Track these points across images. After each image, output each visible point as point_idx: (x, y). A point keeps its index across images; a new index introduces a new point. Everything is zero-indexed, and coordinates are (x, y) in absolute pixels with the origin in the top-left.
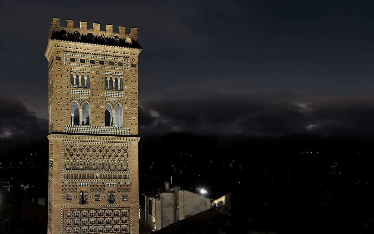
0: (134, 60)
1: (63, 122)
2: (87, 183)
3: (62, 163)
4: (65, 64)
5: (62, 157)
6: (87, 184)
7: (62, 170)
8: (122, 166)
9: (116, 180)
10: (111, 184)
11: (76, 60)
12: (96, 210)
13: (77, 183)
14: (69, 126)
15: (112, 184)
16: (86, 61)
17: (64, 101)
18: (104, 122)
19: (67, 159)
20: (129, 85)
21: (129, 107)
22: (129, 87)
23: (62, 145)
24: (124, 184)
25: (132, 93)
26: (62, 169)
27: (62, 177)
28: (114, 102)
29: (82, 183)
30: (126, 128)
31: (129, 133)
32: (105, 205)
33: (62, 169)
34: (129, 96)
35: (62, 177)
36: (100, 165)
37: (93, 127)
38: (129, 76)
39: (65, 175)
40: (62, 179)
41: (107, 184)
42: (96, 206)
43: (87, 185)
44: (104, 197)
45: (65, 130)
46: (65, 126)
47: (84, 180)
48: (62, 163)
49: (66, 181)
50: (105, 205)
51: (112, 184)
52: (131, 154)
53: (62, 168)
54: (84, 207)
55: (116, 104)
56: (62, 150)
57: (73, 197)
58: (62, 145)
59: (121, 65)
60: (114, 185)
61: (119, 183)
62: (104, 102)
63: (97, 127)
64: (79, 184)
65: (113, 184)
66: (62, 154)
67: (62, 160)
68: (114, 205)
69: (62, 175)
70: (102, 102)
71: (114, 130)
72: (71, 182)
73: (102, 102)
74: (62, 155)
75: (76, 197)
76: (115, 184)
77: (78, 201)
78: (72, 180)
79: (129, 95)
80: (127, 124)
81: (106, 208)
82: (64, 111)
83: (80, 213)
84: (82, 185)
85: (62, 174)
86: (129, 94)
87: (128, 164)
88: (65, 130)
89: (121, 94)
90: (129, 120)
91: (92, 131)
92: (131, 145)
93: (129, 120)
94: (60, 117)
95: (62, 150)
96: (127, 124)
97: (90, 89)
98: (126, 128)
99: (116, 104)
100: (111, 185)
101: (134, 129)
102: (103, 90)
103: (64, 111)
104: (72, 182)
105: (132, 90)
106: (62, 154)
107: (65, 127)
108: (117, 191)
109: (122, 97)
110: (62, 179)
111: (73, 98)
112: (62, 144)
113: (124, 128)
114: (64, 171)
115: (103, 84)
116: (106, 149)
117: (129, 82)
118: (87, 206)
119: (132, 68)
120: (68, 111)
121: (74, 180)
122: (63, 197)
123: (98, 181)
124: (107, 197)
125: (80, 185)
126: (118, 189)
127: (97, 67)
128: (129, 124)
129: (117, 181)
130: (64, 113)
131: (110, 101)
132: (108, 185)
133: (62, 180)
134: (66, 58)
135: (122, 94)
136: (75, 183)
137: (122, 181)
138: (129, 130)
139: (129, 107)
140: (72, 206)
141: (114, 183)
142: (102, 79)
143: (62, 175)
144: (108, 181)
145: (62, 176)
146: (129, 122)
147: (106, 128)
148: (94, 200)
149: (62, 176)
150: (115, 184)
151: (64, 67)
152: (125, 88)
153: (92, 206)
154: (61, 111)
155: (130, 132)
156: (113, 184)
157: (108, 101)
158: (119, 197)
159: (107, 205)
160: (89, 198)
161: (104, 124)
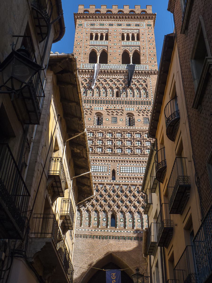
18: (121, 61)
46: (82, 64)
59: (137, 25)
76: (133, 109)
113: (141, 65)
115: (120, 37)
147: (123, 65)
150: (133, 109)
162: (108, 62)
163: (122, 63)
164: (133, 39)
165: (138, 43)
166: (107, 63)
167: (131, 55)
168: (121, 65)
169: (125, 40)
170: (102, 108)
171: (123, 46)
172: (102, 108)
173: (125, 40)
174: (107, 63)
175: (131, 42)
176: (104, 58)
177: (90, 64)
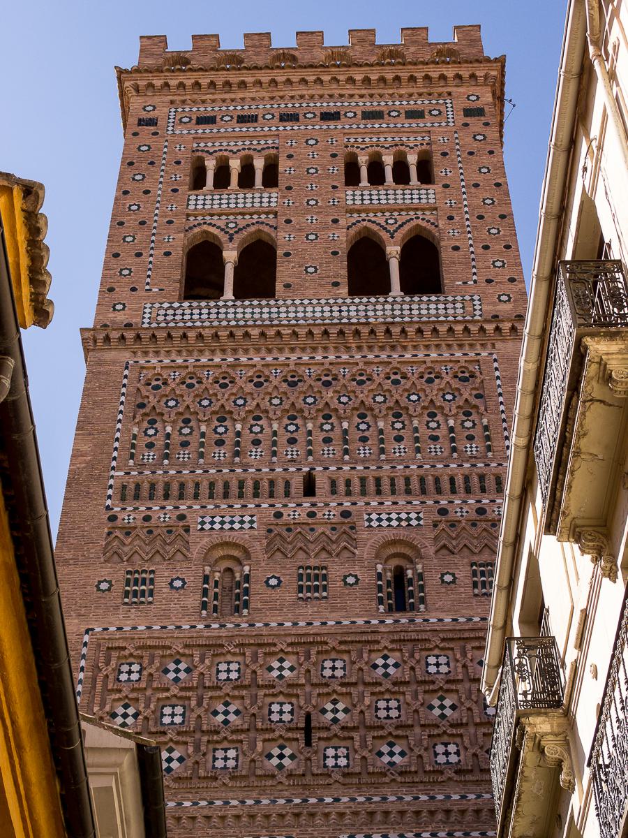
0: (473, 98)
1: (140, 293)
2: (247, 519)
3: (117, 439)
4: (170, 132)
5: (120, 417)
6: (252, 522)
7: (113, 468)
8: (453, 440)
9: (423, 498)
10: (394, 516)
11: (218, 119)
12: (305, 644)
13: (194, 520)
14: (166, 305)
15: (399, 519)
16: (260, 118)
17: (154, 231)
18: (344, 282)
19: (145, 424)
20: (460, 165)
21: (469, 229)
22: (461, 171)
23: (126, 372)
24: (474, 516)
25: (476, 185)
26: (114, 463)
27: (109, 497)
28: (391, 221)
29: (218, 519)
30: (459, 298)
31: (478, 313)
32: (360, 621)
33: (114, 463)
34: (465, 196)
35: (109, 497)
36: (327, 441)
37: (289, 302)
38: (457, 141)
39: (124, 487)
40: (109, 502)
41: (370, 520)
42: (302, 624)
43: (247, 526)
44: (351, 580)
45: (146, 321)
47: (231, 506)
48: (117, 439)
49: (130, 514)
50: (360, 621)
51: (399, 519)
52: (500, 390)
53: (115, 459)
54: (223, 633)
55: (401, 226)
56: (124, 390)
57: (161, 586)
58: (126, 372)
60: (414, 523)
61: (443, 512)
62: (343, 222)
63: (306, 302)
64: (203, 523)
65: (403, 516)
66: (122, 403)
67: (119, 426)
68: (419, 620)
69: (111, 487)
70: (335, 221)
71: (397, 307)
72: (155, 517)
73: (335, 221)
74: (121, 408)
75: (178, 584)
76: (418, 519)
77: (193, 600)
78: (163, 508)
79: (464, 193)
80: (465, 283)
81: (366, 640)
82: (151, 259)
83: (202, 661)
84: (217, 526)
85: (111, 482)
86: (464, 190)
87: (486, 428)
88: (146, 321)
89: (423, 192)
90: (474, 270)
91: (283, 315)
92: (495, 356)
93: (474, 270)
94: (126, 280)
95: (124, 390)
96: (465, 283)
97: (274, 190)
98: (459, 298)
99: (401, 226)
100: (394, 523)
101: (504, 298)
102: (334, 187)
103: (151, 259)
104: (163, 512)
105: (479, 179)
106: (122, 403)
107: (148, 310)
108: (432, 550)
109: (432, 201)
110: (109, 502)
111: (196, 223)
112: (127, 368)
113: (450, 299)
114: (121, 470)
115: (339, 169)
116: (359, 378)
117: (459, 156)
118: (244, 625)
119: (468, 120)
120: (166, 259)
121: (176, 508)
122: (100, 582)
123: (313, 505)
124: (367, 579)
125: (207, 527)
126: (436, 538)
127: (310, 127)
128: (475, 282)
129: (430, 502)
130: (151, 266)
131: (373, 219)
132: (375, 524)
133: (108, 508)
134: (178, 117)
135: (431, 191)
136: (182, 517)
137: (462, 507)
138: (477, 303)
139: (469, 229)
140: (149, 628)
141: (413, 515)
142: (334, 156)
143: (111, 487)
144: (374, 504)
145: (110, 492)
146: (475, 277)
147: (357, 300)
148: (288, 595)
149: (110, 492)
150: (418, 519)
151: (167, 141)
152: (439, 171)
153: (273, 624)
154: (138, 260)
155: (485, 307)
156: (403, 516)
157: (364, 220)
158: (448, 578)
159: (375, 622)
160: (256, 586)
161: (344, 291)
162: (279, 286)
163: (353, 292)
164: (401, 175)
165: (429, 195)
166: (269, 293)
167: (393, 251)
168: (348, 301)
169: (364, 182)
170: (244, 521)
171: (351, 212)
172: (244, 521)
173: (364, 182)
174: (269, 293)
175: (390, 194)
176: (259, 271)
177: (186, 304)
